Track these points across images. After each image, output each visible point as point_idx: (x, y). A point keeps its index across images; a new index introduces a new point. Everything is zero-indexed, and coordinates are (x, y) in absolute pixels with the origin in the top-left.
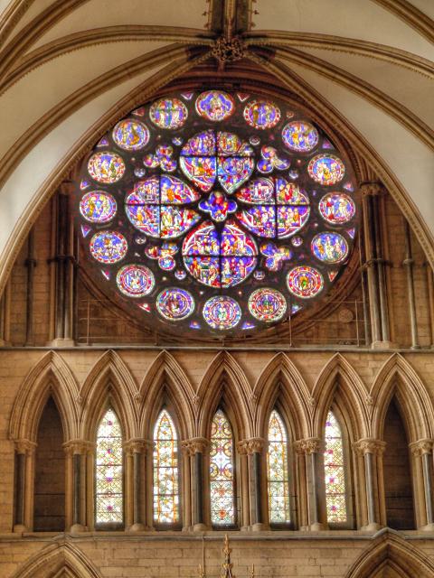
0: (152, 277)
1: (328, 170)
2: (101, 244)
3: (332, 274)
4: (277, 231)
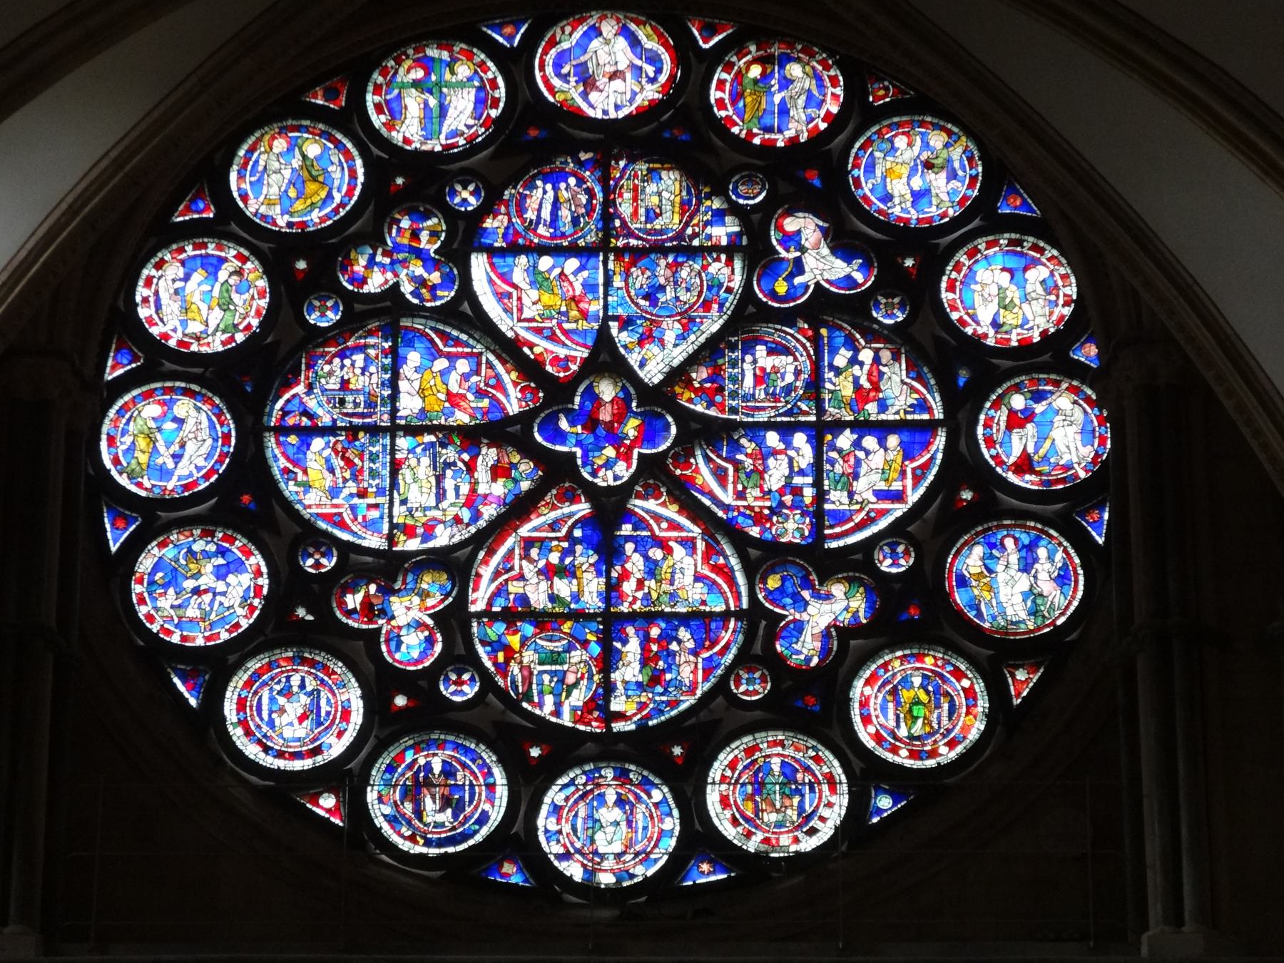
0: (353, 696)
1: (1013, 293)
2: (173, 580)
3: (1021, 675)
4: (817, 528)
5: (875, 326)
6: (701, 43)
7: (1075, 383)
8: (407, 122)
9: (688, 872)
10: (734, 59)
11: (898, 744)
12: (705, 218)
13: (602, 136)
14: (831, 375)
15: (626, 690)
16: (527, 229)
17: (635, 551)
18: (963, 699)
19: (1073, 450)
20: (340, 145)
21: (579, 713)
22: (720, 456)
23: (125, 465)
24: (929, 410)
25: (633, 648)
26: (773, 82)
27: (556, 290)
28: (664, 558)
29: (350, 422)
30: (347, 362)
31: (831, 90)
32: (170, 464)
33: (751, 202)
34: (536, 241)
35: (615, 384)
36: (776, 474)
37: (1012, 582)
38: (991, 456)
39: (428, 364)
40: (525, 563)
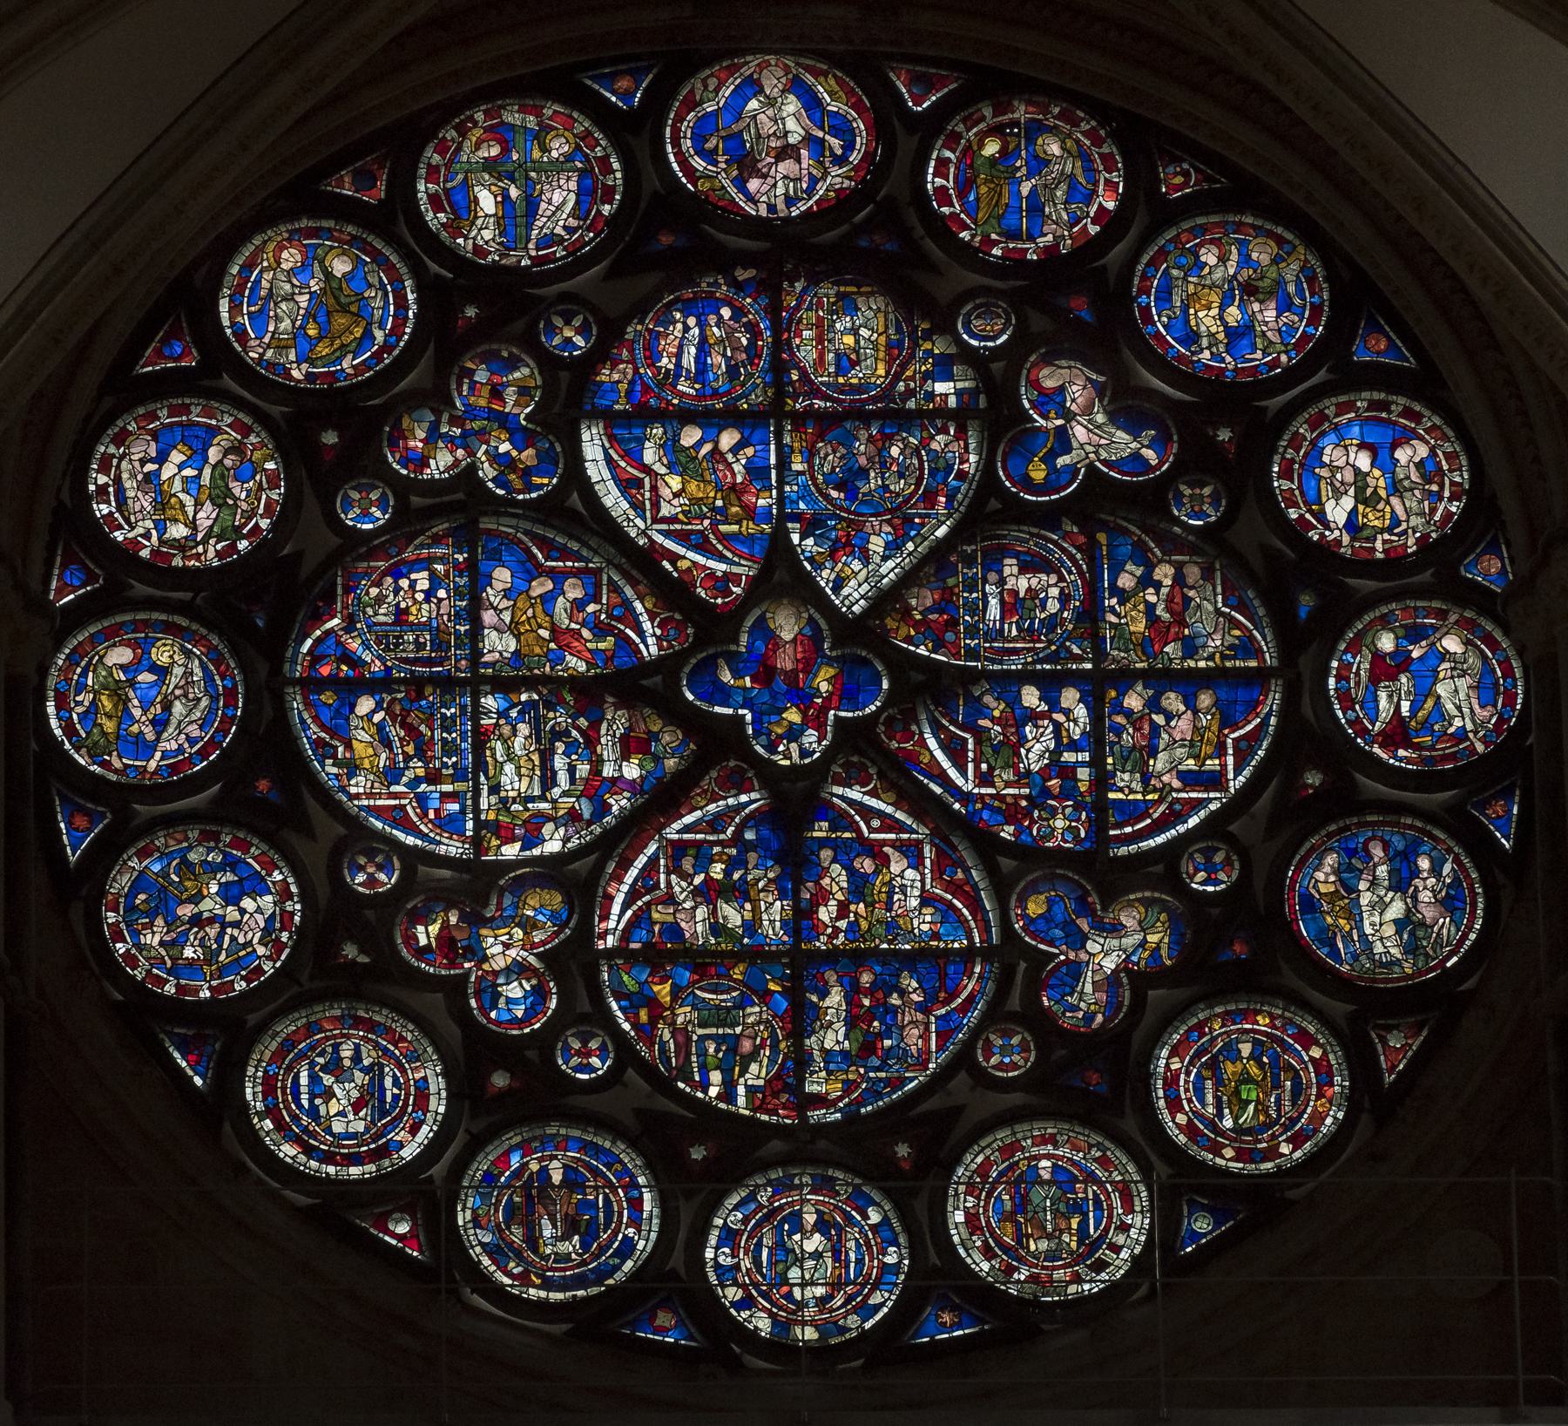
1: (1378, 480)
2: (163, 903)
3: (1395, 1042)
4: (1098, 827)
5: (1177, 529)
7: (1468, 614)
8: (479, 222)
9: (923, 1323)
10: (961, 128)
12: (923, 368)
13: (768, 245)
14: (1114, 601)
15: (827, 1062)
16: (660, 385)
17: (834, 860)
19: (1466, 711)
21: (760, 1096)
22: (954, 722)
24: (1258, 654)
28: (877, 872)
29: (412, 672)
30: (404, 583)
32: (150, 736)
33: (990, 344)
34: (675, 401)
35: (799, 617)
37: (1383, 906)
40: (673, 877)
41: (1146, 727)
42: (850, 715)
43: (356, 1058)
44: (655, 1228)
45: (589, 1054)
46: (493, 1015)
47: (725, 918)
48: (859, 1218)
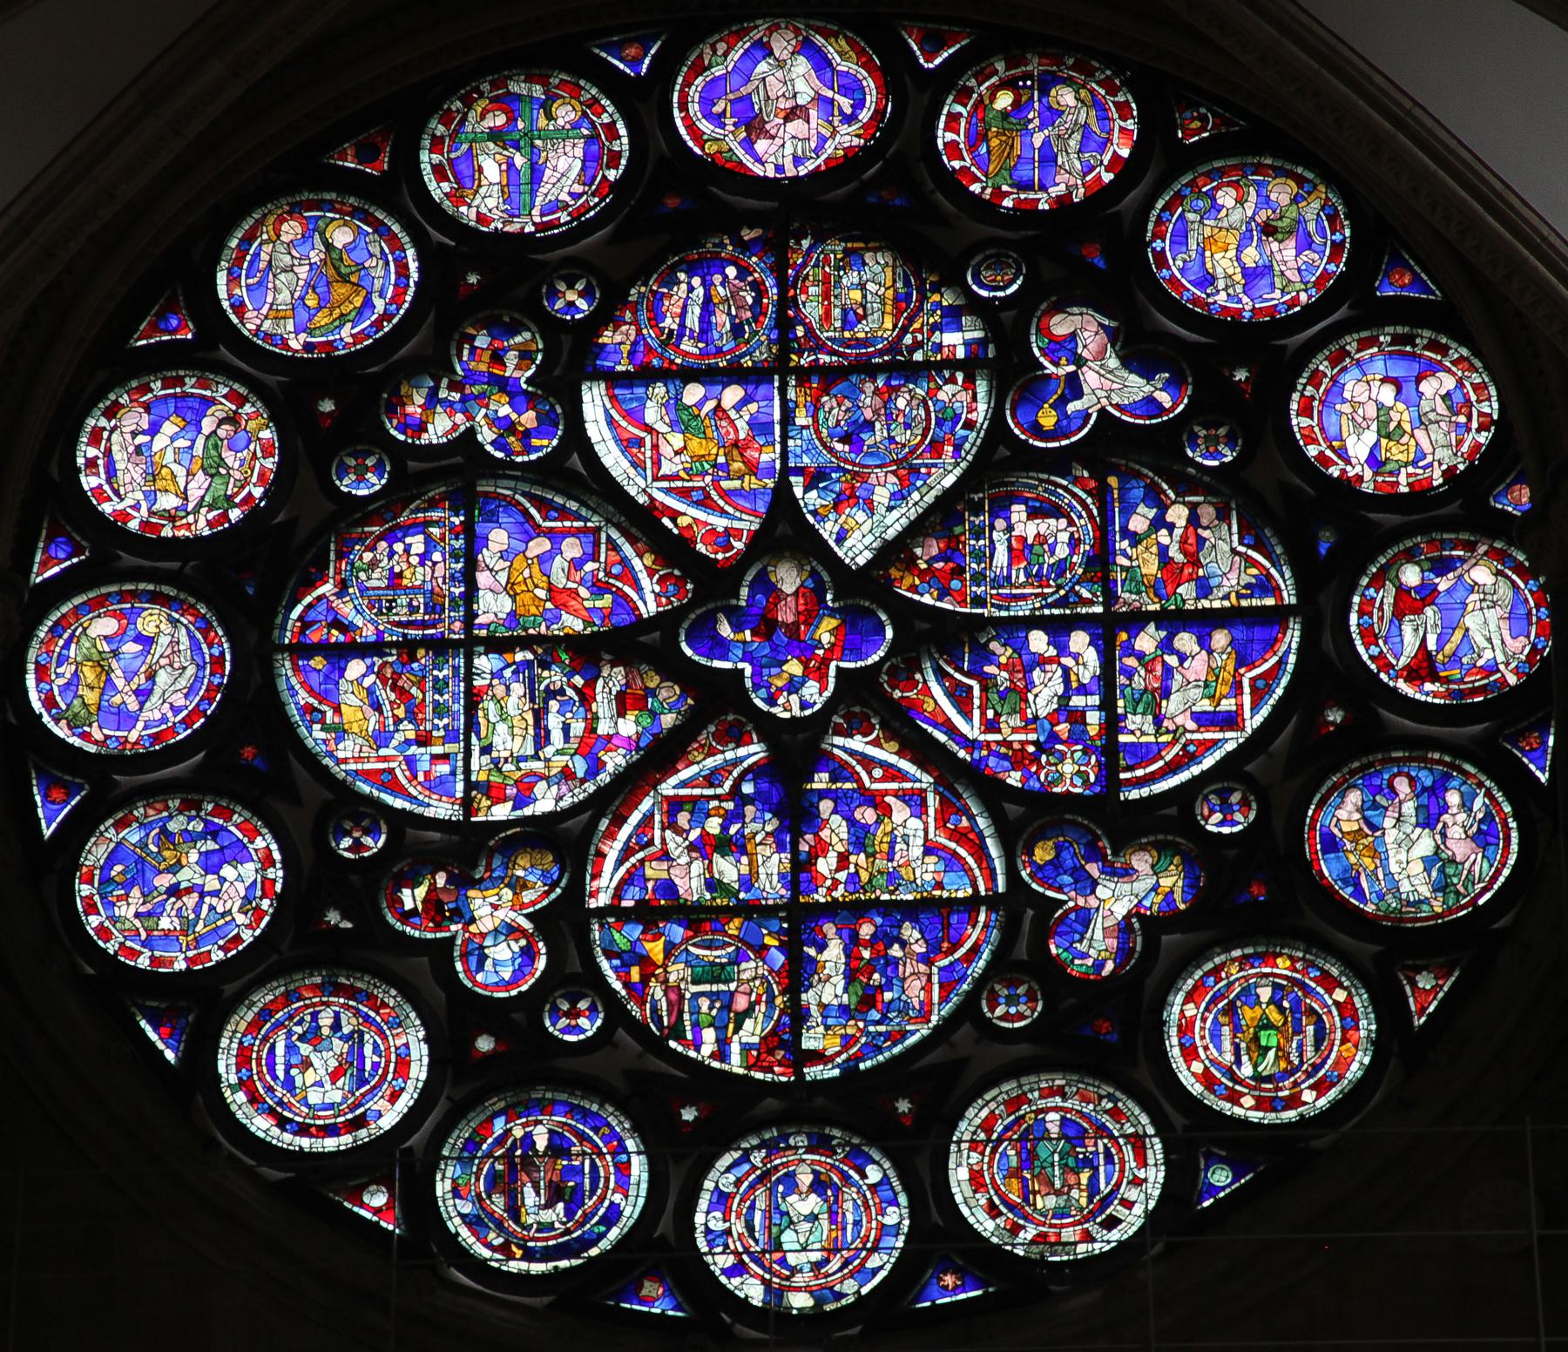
1: (1401, 414)
2: (139, 875)
3: (1425, 982)
4: (1109, 771)
5: (1191, 470)
6: (922, 61)
7: (1498, 545)
8: (483, 191)
9: (925, 1286)
10: (973, 83)
11: (1238, 1087)
13: (775, 204)
14: (1125, 544)
15: (825, 1017)
16: (664, 344)
17: (835, 811)
18: (1337, 1019)
19: (1497, 642)
20: (382, 229)
21: (754, 1053)
22: (960, 670)
23: (63, 707)
24: (1276, 591)
25: (833, 954)
26: (1031, 116)
27: (708, 431)
28: (878, 822)
29: (404, 635)
30: (399, 547)
31: (1119, 123)
32: (132, 704)
33: (1000, 294)
34: (678, 361)
35: (800, 569)
36: (1045, 694)
38: (1372, 657)
39: (521, 546)
40: (668, 833)
41: (1159, 668)
42: (851, 665)
43: (336, 1026)
44: (643, 1193)
45: (578, 1014)
46: (480, 977)
47: (720, 873)
48: (856, 1177)
